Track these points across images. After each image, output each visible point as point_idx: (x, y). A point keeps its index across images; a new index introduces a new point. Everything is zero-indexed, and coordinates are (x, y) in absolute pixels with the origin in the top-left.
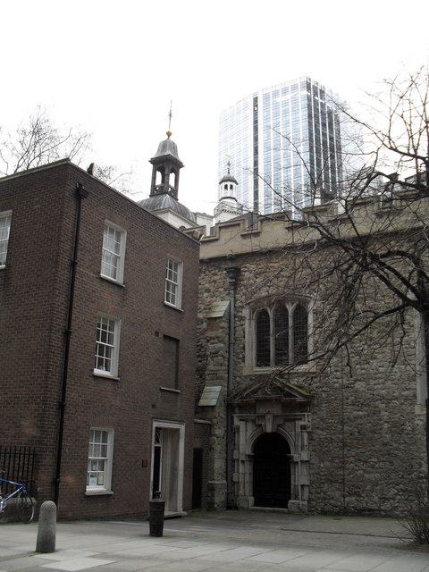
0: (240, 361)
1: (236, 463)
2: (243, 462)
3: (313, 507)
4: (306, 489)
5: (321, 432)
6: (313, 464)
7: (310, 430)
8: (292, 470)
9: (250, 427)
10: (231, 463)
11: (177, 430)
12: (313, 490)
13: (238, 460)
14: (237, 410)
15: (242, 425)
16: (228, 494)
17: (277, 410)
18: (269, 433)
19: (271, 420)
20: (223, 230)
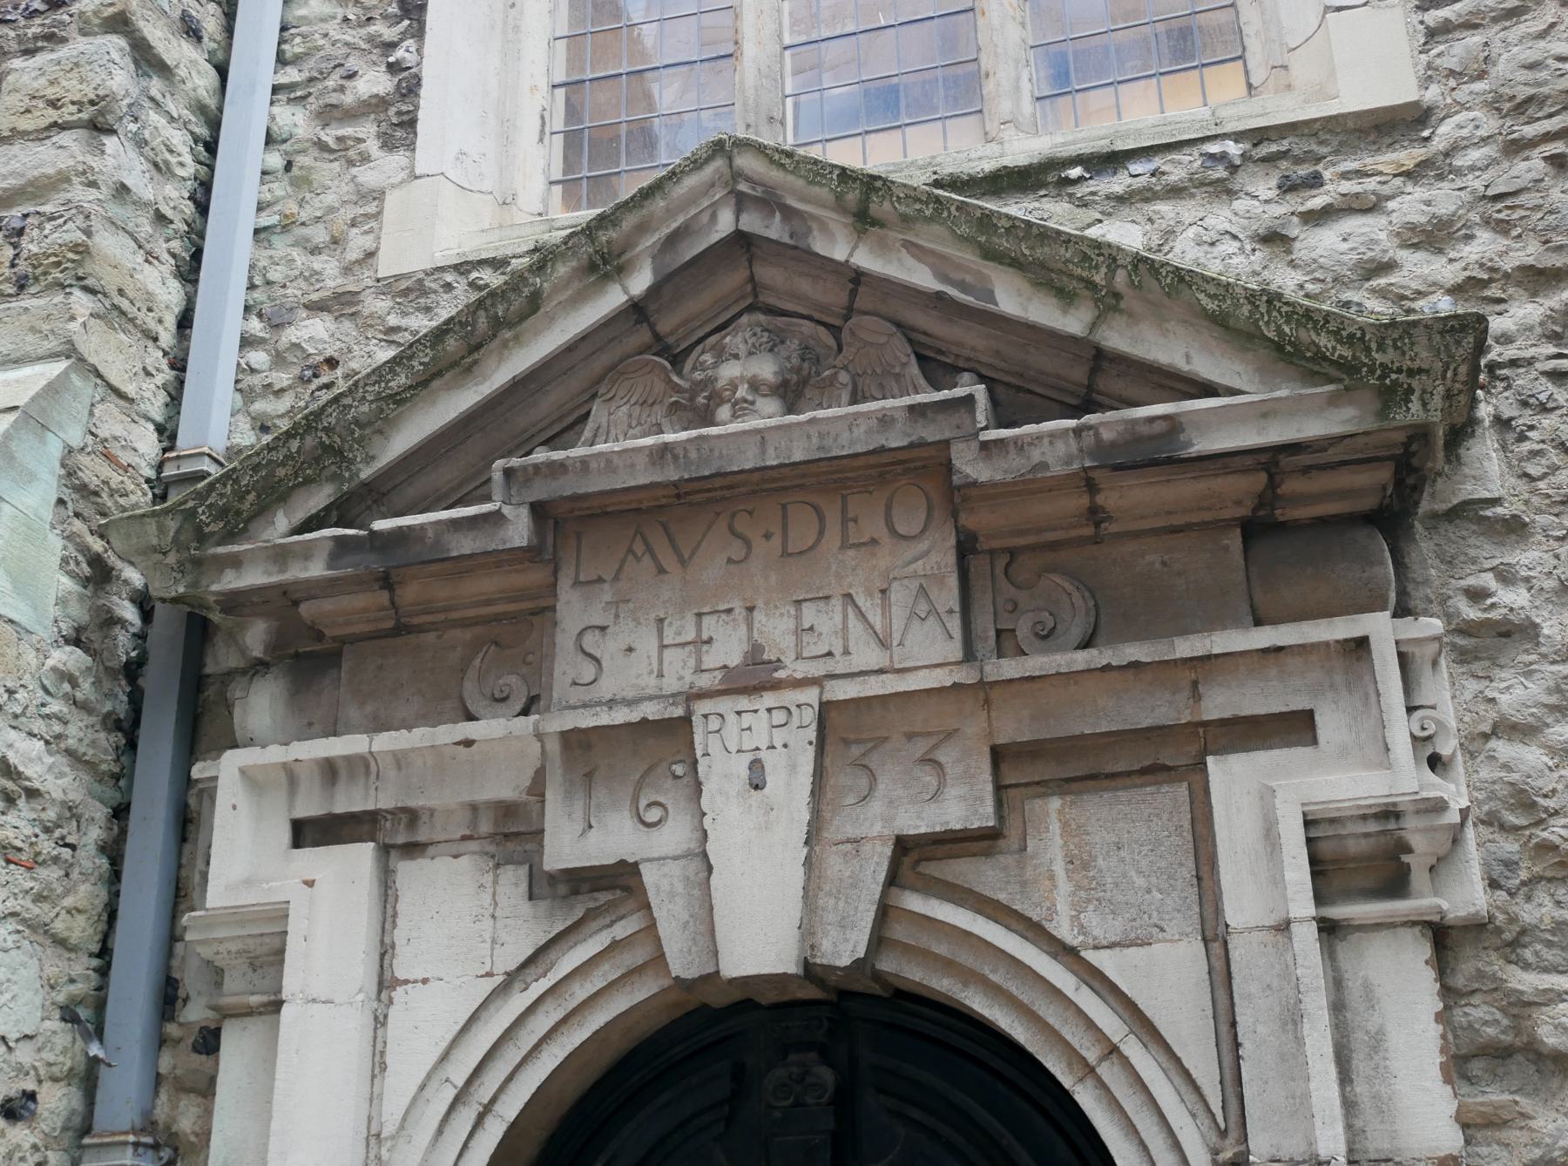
0: (367, 130)
9: (464, 924)
14: (260, 706)
17: (887, 624)
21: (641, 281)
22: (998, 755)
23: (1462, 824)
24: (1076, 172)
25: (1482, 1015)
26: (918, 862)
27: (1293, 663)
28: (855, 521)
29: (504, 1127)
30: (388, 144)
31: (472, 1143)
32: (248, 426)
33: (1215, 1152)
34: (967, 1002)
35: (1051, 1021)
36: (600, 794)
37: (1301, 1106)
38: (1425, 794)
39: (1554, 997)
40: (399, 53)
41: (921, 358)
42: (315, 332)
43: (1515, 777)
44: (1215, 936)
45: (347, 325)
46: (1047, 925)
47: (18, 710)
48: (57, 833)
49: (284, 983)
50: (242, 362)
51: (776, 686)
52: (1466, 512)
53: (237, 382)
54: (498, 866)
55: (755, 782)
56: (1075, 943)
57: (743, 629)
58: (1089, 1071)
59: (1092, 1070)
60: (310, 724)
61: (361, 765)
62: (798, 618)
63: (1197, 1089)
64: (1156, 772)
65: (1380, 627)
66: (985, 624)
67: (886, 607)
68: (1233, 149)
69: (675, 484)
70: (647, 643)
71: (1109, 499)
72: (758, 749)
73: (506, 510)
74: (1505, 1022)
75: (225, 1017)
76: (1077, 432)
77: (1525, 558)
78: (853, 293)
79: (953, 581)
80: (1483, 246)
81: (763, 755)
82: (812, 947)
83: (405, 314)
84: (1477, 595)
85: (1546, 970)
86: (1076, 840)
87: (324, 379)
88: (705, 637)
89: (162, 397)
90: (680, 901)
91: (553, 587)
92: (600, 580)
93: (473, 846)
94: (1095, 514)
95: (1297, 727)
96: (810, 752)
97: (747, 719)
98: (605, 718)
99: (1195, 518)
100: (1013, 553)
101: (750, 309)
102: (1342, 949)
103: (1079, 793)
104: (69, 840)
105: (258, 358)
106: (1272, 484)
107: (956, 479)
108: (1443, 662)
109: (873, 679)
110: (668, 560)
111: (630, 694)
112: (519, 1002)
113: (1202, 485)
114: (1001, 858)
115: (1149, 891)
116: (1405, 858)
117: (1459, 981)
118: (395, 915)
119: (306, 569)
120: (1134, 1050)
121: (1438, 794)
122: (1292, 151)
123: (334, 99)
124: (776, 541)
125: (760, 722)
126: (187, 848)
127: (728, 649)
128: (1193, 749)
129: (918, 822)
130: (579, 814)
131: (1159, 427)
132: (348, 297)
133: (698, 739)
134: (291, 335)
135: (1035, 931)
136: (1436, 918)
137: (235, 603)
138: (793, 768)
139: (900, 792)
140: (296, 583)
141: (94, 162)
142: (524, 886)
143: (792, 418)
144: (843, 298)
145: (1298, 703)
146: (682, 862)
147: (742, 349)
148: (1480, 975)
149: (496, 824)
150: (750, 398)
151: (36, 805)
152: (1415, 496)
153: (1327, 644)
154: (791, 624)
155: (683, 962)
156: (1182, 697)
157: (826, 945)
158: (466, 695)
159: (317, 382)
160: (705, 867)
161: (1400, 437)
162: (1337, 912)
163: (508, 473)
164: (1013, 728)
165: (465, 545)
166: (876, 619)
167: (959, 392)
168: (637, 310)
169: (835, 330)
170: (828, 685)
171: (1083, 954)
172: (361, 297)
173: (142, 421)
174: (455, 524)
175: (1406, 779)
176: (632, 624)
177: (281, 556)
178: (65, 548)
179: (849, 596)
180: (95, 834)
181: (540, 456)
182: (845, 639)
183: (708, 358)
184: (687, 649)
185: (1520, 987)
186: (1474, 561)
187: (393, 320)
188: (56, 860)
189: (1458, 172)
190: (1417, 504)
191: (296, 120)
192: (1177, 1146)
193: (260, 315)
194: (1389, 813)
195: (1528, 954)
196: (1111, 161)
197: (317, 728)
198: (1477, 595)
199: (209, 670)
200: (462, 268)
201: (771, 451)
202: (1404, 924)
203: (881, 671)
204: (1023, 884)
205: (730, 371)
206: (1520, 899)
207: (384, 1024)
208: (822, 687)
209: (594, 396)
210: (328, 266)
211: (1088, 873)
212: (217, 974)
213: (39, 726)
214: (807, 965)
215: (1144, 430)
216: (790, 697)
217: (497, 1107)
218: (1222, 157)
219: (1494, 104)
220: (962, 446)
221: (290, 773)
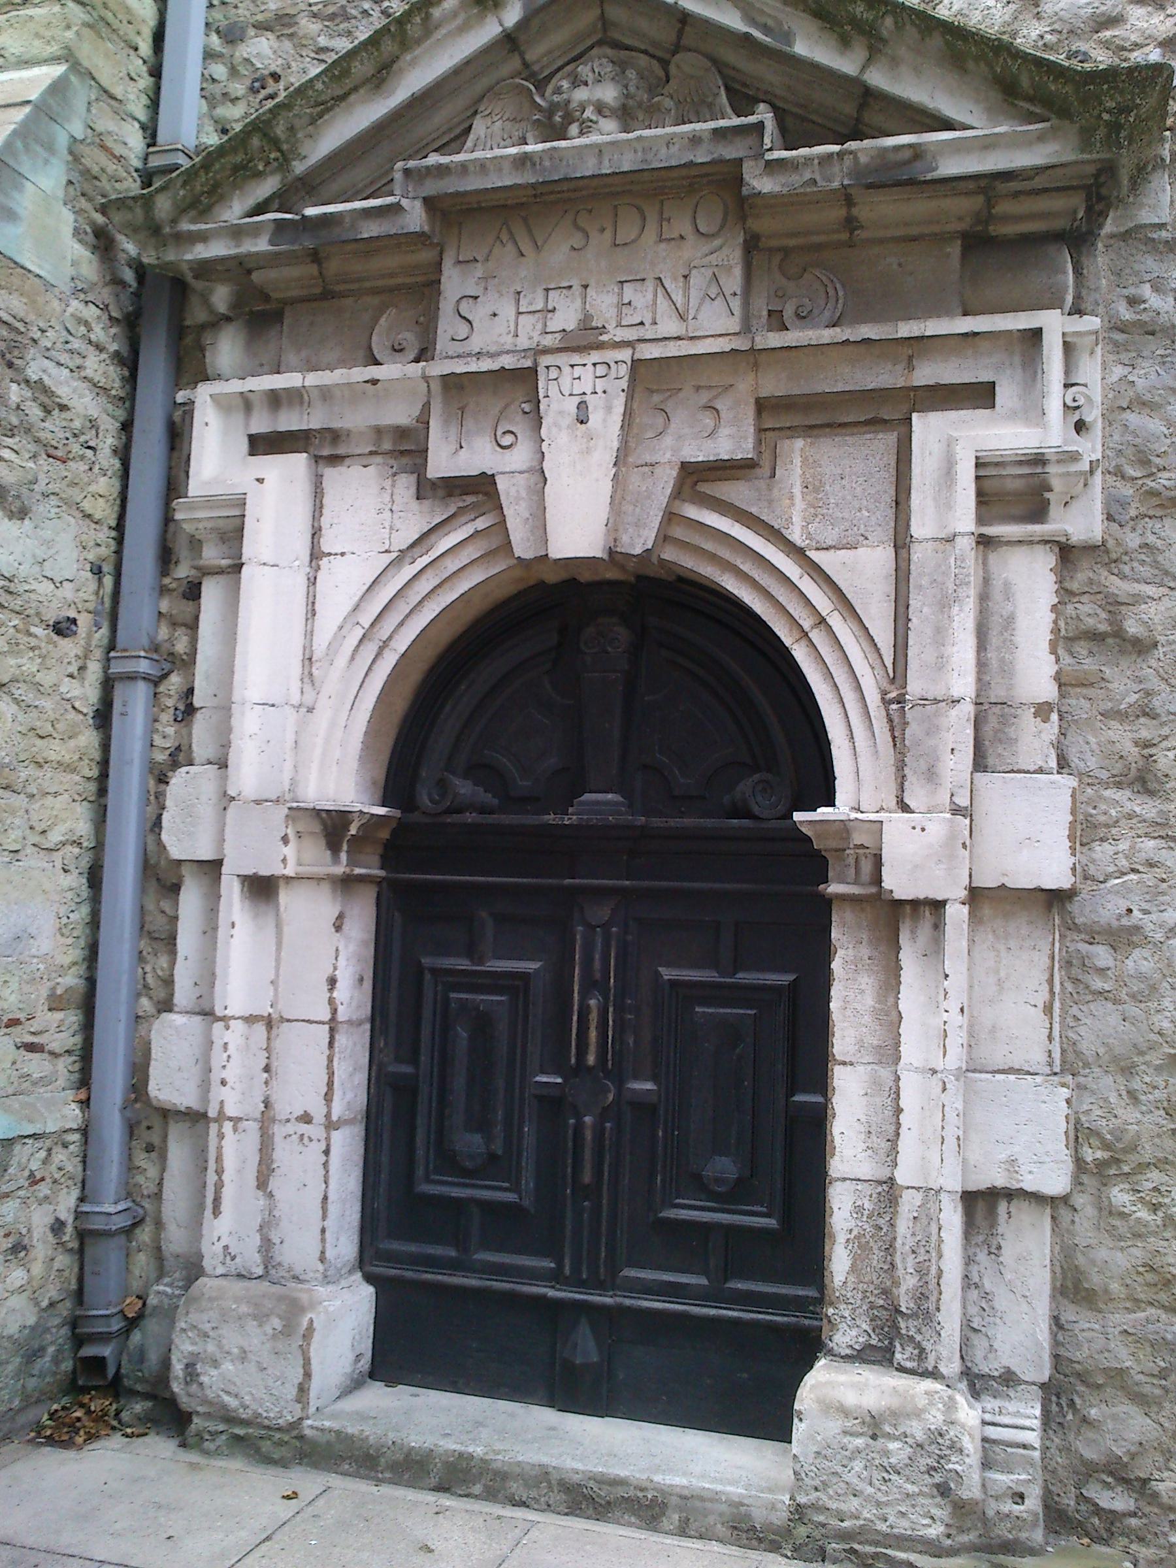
1: (190, 901)
2: (262, 888)
3: (1117, 1472)
4: (1028, 1246)
6: (1123, 937)
7: (1082, 521)
9: (370, 514)
12: (1111, 1262)
13: (212, 868)
14: (226, 350)
16: (84, 1239)
19: (607, 422)
22: (762, 406)
23: (1092, 472)
26: (696, 484)
27: (984, 345)
28: (669, 220)
29: (397, 657)
31: (375, 667)
32: (212, 129)
33: (884, 693)
34: (723, 584)
35: (780, 599)
36: (469, 423)
38: (1066, 448)
39: (1138, 599)
41: (728, 89)
42: (262, 50)
43: (1138, 441)
44: (902, 542)
45: (287, 45)
46: (784, 531)
47: (49, 345)
48: (82, 439)
49: (244, 550)
50: (205, 72)
51: (600, 346)
53: (202, 89)
54: (394, 475)
55: (581, 418)
56: (803, 545)
57: (579, 302)
59: (806, 634)
60: (262, 365)
62: (621, 295)
63: (878, 650)
64: (876, 423)
65: (1054, 324)
66: (761, 306)
67: (687, 289)
69: (533, 186)
70: (507, 310)
71: (862, 212)
72: (584, 393)
73: (405, 203)
74: (1104, 615)
75: (204, 574)
76: (840, 154)
78: (680, 33)
79: (738, 271)
81: (586, 398)
82: (615, 540)
83: (331, 37)
85: (1137, 581)
86: (812, 471)
87: (269, 91)
88: (550, 307)
89: (144, 100)
90: (523, 504)
91: (438, 266)
92: (476, 260)
93: (379, 459)
94: (851, 224)
95: (981, 395)
96: (622, 398)
97: (578, 371)
98: (473, 367)
99: (926, 230)
100: (786, 252)
101: (600, 43)
102: (993, 557)
103: (817, 437)
104: (91, 444)
105: (219, 70)
106: (989, 204)
107: (745, 191)
108: (1099, 350)
109: (672, 343)
110: (526, 246)
111: (493, 349)
112: (408, 571)
113: (933, 205)
114: (756, 482)
115: (860, 510)
116: (1047, 495)
117: (1074, 586)
118: (321, 507)
119: (256, 245)
120: (836, 622)
121: (1075, 448)
124: (608, 234)
125: (587, 374)
126: (175, 454)
127: (566, 317)
128: (905, 408)
130: (453, 438)
131: (907, 154)
132: (286, 20)
133: (541, 384)
134: (244, 51)
135: (776, 536)
136: (1063, 539)
137: (205, 269)
138: (609, 409)
139: (686, 430)
140: (249, 255)
142: (413, 490)
143: (624, 136)
144: (673, 37)
145: (985, 377)
146: (526, 475)
147: (590, 78)
148: (1091, 582)
149: (394, 444)
150: (594, 118)
151: (64, 415)
152: (1101, 220)
153: (1011, 331)
154: (614, 299)
155: (523, 548)
156: (899, 368)
157: (625, 539)
158: (374, 345)
159: (264, 93)
160: (542, 480)
161: (1090, 169)
162: (992, 530)
163: (407, 172)
164: (774, 385)
165: (371, 229)
166: (678, 298)
167: (752, 119)
168: (510, 41)
169: (665, 64)
170: (641, 347)
171: (807, 553)
172: (298, 19)
173: (130, 120)
174: (367, 213)
175: (1050, 434)
176: (496, 295)
177: (237, 233)
178: (76, 221)
179: (660, 279)
181: (434, 159)
182: (654, 313)
183: (565, 84)
184: (537, 315)
185: (1116, 592)
186: (1137, 274)
187: (323, 41)
188: (82, 457)
190: (1101, 226)
192: (858, 688)
193: (218, 32)
194: (1038, 460)
195: (1126, 569)
197: (266, 368)
198: (1133, 301)
199: (188, 323)
201: (606, 162)
202: (1039, 542)
203: (679, 338)
204: (770, 502)
205: (581, 94)
206: (1127, 529)
207: (314, 584)
208: (634, 349)
209: (476, 113)
211: (819, 493)
212: (196, 544)
213: (64, 358)
214: (611, 552)
215: (892, 157)
216: (611, 355)
217: (393, 644)
220: (752, 163)
221: (246, 402)
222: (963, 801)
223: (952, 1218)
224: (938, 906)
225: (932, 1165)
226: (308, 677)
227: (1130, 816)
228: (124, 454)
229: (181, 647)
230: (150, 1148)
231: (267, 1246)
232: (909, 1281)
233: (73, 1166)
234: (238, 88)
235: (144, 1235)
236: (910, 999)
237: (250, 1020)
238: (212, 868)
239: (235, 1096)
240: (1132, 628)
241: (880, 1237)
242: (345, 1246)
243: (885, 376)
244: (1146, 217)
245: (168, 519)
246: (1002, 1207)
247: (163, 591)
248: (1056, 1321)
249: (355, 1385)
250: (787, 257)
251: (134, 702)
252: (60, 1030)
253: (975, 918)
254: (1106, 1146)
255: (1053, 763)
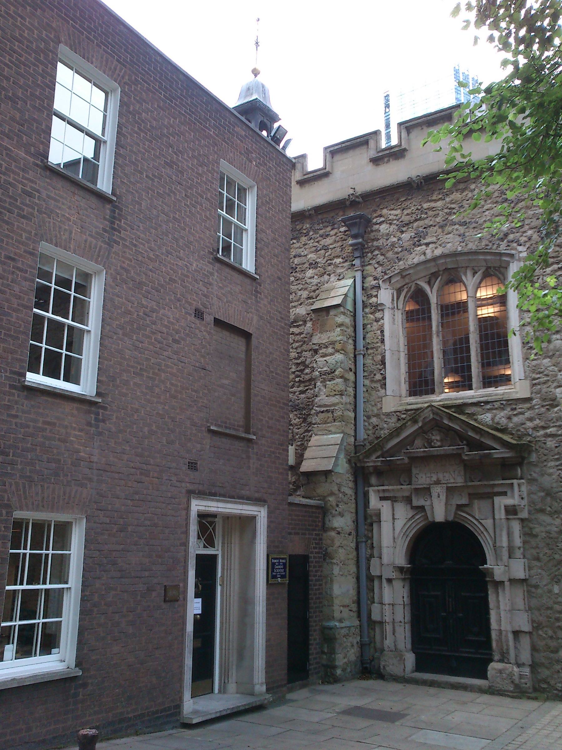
0: (378, 385)
1: (376, 583)
2: (389, 581)
3: (545, 681)
4: (525, 642)
5: (547, 519)
6: (536, 587)
8: (492, 598)
9: (403, 512)
10: (366, 583)
11: (252, 519)
12: (541, 644)
13: (380, 577)
14: (373, 480)
15: (385, 508)
16: (362, 646)
18: (440, 523)
19: (443, 497)
20: (337, 157)
21: (420, 424)
22: (469, 494)
24: (482, 404)
25: (526, 529)
30: (382, 388)
37: (501, 541)
39: (534, 528)
40: (382, 372)
42: (374, 420)
44: (494, 519)
45: (379, 420)
52: (530, 463)
58: (480, 535)
61: (388, 490)
65: (515, 482)
68: (504, 402)
70: (424, 477)
77: (537, 470)
80: (537, 422)
84: (531, 475)
95: (505, 494)
120: (485, 533)
122: (512, 403)
123: (373, 379)
127: (434, 478)
129: (459, 503)
141: (341, 400)
155: (430, 519)
164: (471, 491)
165: (398, 462)
177: (375, 462)
180: (354, 497)
187: (385, 420)
189: (535, 409)
191: (367, 382)
194: (514, 506)
196: (487, 403)
198: (531, 475)
200: (395, 412)
205: (433, 438)
210: (375, 409)
211: (479, 509)
212: (371, 516)
214: (446, 520)
218: (502, 404)
219: (541, 398)
221: (378, 491)
222: (506, 564)
223: (511, 636)
224: (504, 582)
225: (506, 626)
226: (394, 541)
227: (536, 566)
228: (356, 499)
229: (370, 535)
230: (372, 629)
231: (395, 645)
232: (505, 647)
233: (359, 632)
234: (371, 428)
235: (372, 645)
236: (501, 598)
237: (389, 604)
238: (380, 577)
239: (387, 619)
240: (534, 533)
241: (499, 640)
242: (409, 646)
243: (489, 490)
244: (532, 460)
245: (365, 511)
246: (520, 634)
247: (365, 524)
248: (532, 655)
249: (413, 672)
250: (471, 469)
251: (363, 546)
252: (354, 607)
253: (511, 584)
254: (537, 623)
255: (522, 557)
